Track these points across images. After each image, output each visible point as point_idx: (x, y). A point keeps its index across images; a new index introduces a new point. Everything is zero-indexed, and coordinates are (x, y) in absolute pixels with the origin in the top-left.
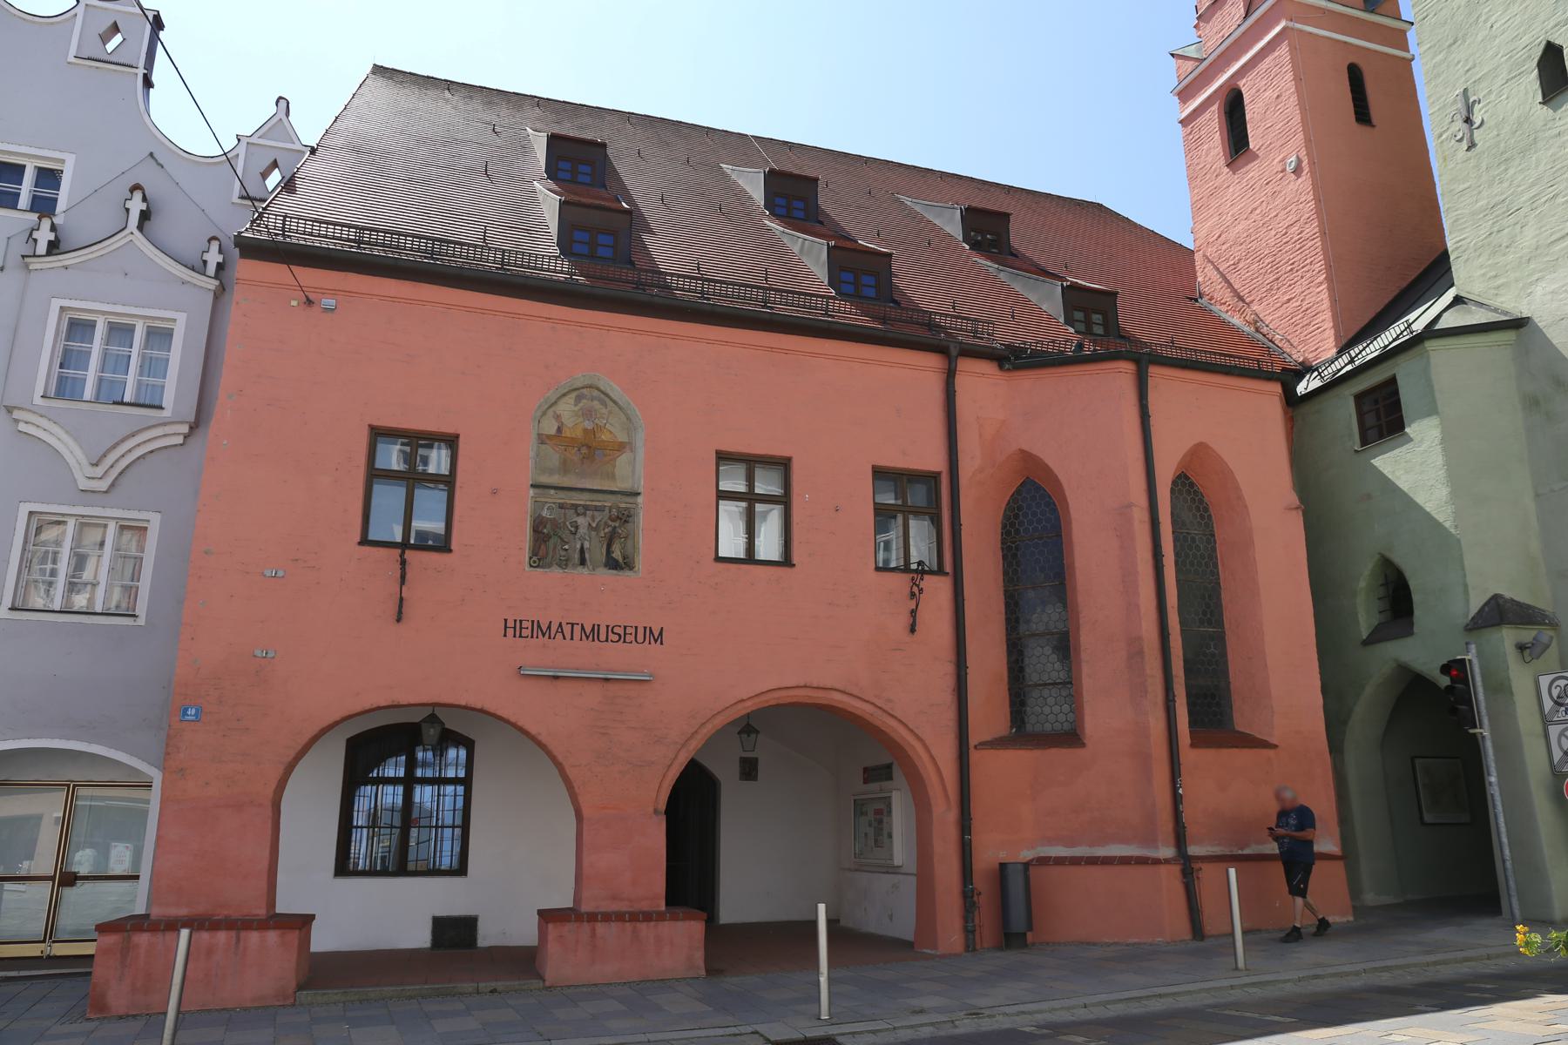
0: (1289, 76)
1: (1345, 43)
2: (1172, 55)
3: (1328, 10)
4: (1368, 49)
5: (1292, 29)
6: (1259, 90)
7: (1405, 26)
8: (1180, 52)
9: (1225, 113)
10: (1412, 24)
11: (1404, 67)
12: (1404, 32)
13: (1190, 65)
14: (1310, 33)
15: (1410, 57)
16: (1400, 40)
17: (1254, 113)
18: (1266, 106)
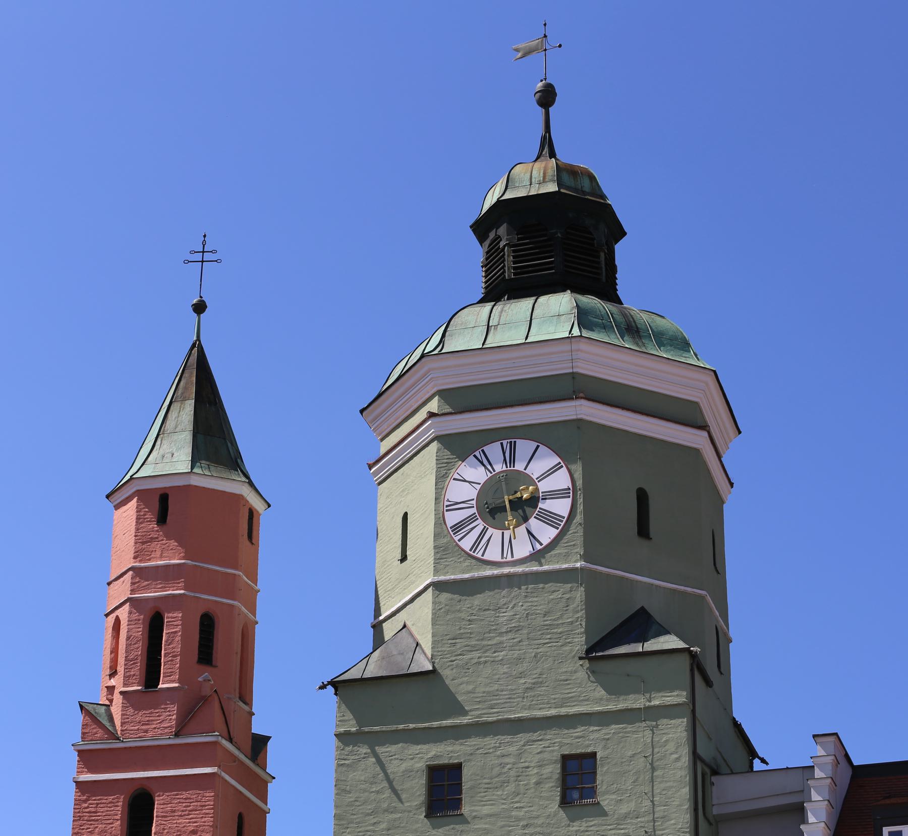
0: (209, 820)
1: (240, 792)
2: (82, 707)
3: (238, 759)
4: (249, 799)
5: (219, 776)
6: (174, 811)
7: (267, 778)
8: (90, 708)
9: (129, 805)
10: (274, 778)
11: (262, 814)
12: (265, 784)
13: (100, 733)
14: (226, 781)
15: (268, 811)
16: (260, 786)
17: (164, 829)
18: (178, 831)
